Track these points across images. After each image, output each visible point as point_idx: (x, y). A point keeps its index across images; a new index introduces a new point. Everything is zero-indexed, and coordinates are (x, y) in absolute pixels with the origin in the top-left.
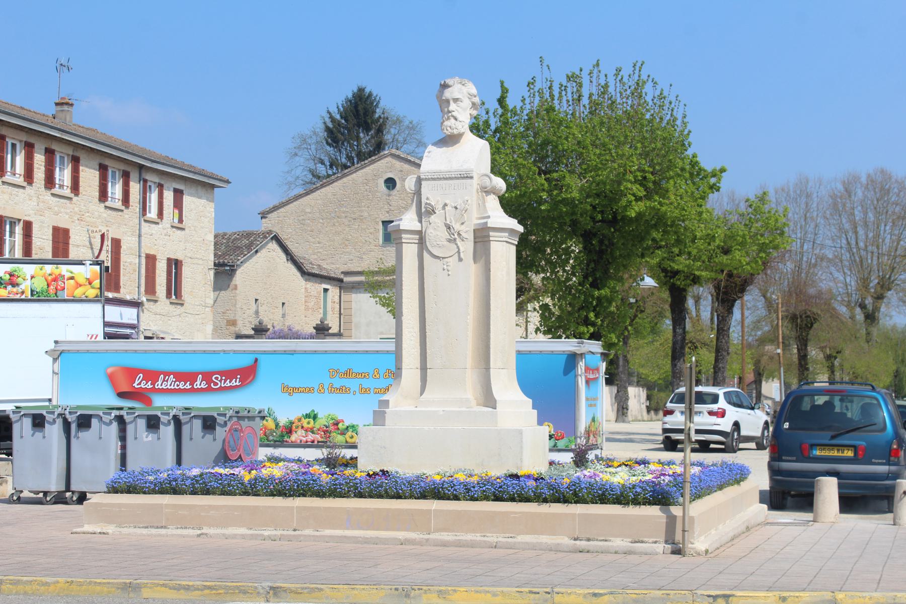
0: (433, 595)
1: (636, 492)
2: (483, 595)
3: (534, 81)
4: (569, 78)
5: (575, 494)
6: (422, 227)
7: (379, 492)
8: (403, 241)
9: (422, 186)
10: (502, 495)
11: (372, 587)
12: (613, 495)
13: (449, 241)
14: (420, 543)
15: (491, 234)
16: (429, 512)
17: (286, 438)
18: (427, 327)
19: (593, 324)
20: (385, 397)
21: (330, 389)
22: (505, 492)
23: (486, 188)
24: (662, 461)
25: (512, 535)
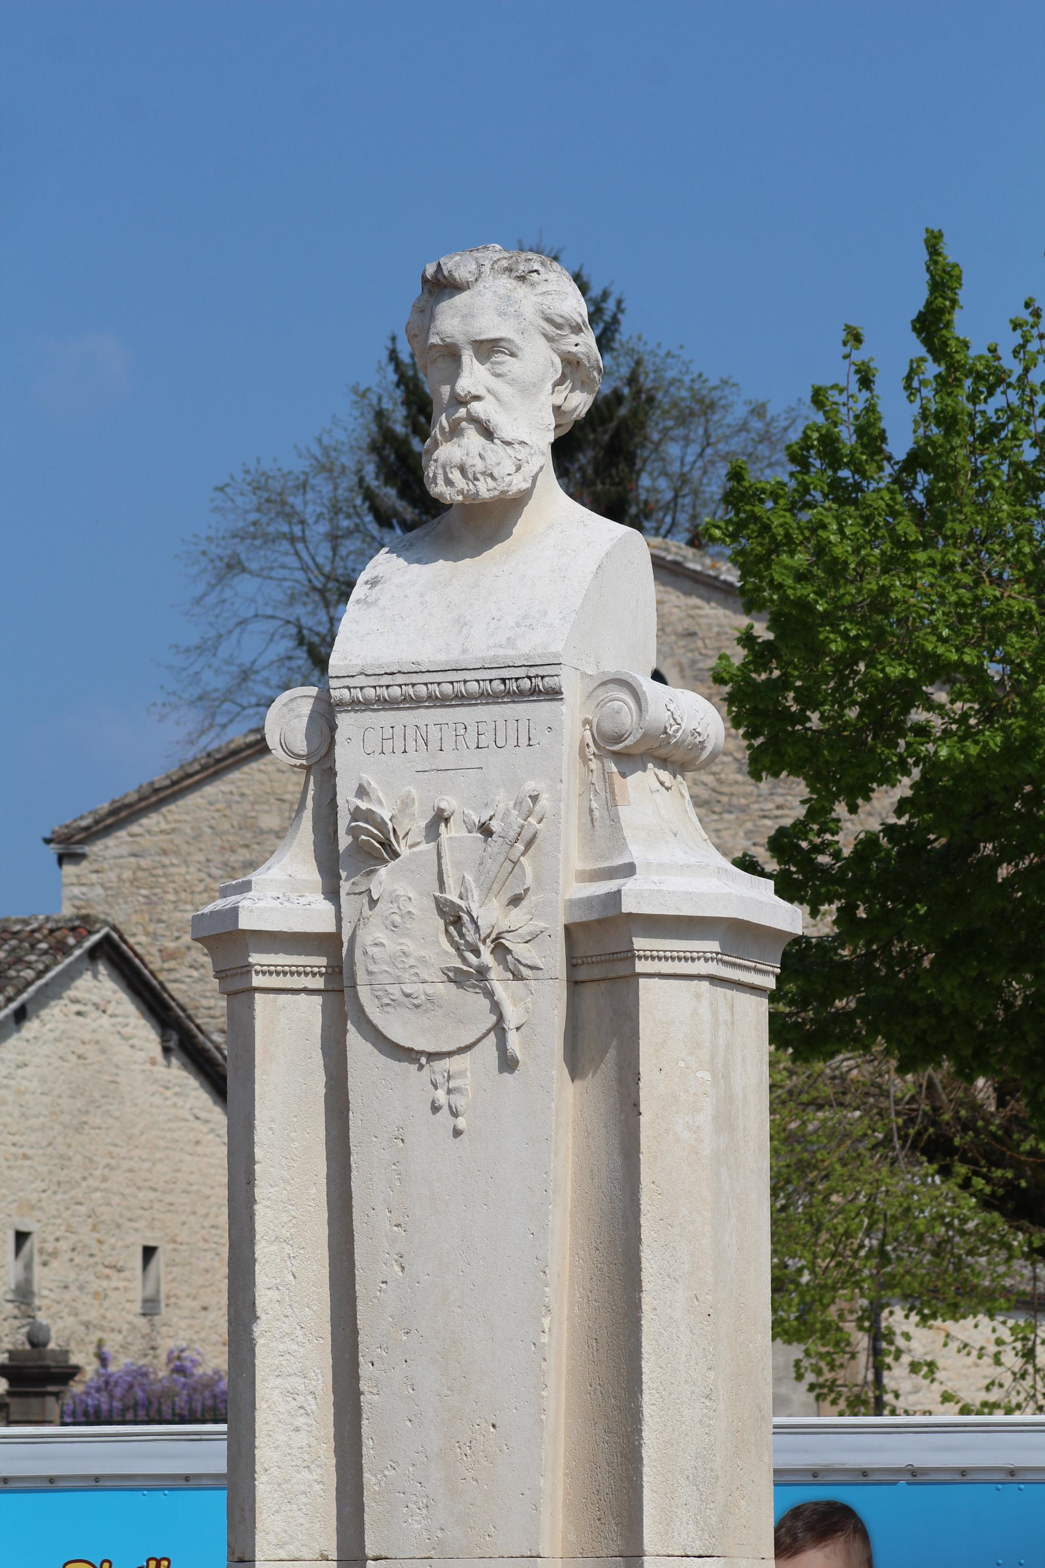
6: (339, 919)
8: (257, 981)
13: (458, 978)
15: (640, 943)
18: (365, 1370)
23: (619, 739)
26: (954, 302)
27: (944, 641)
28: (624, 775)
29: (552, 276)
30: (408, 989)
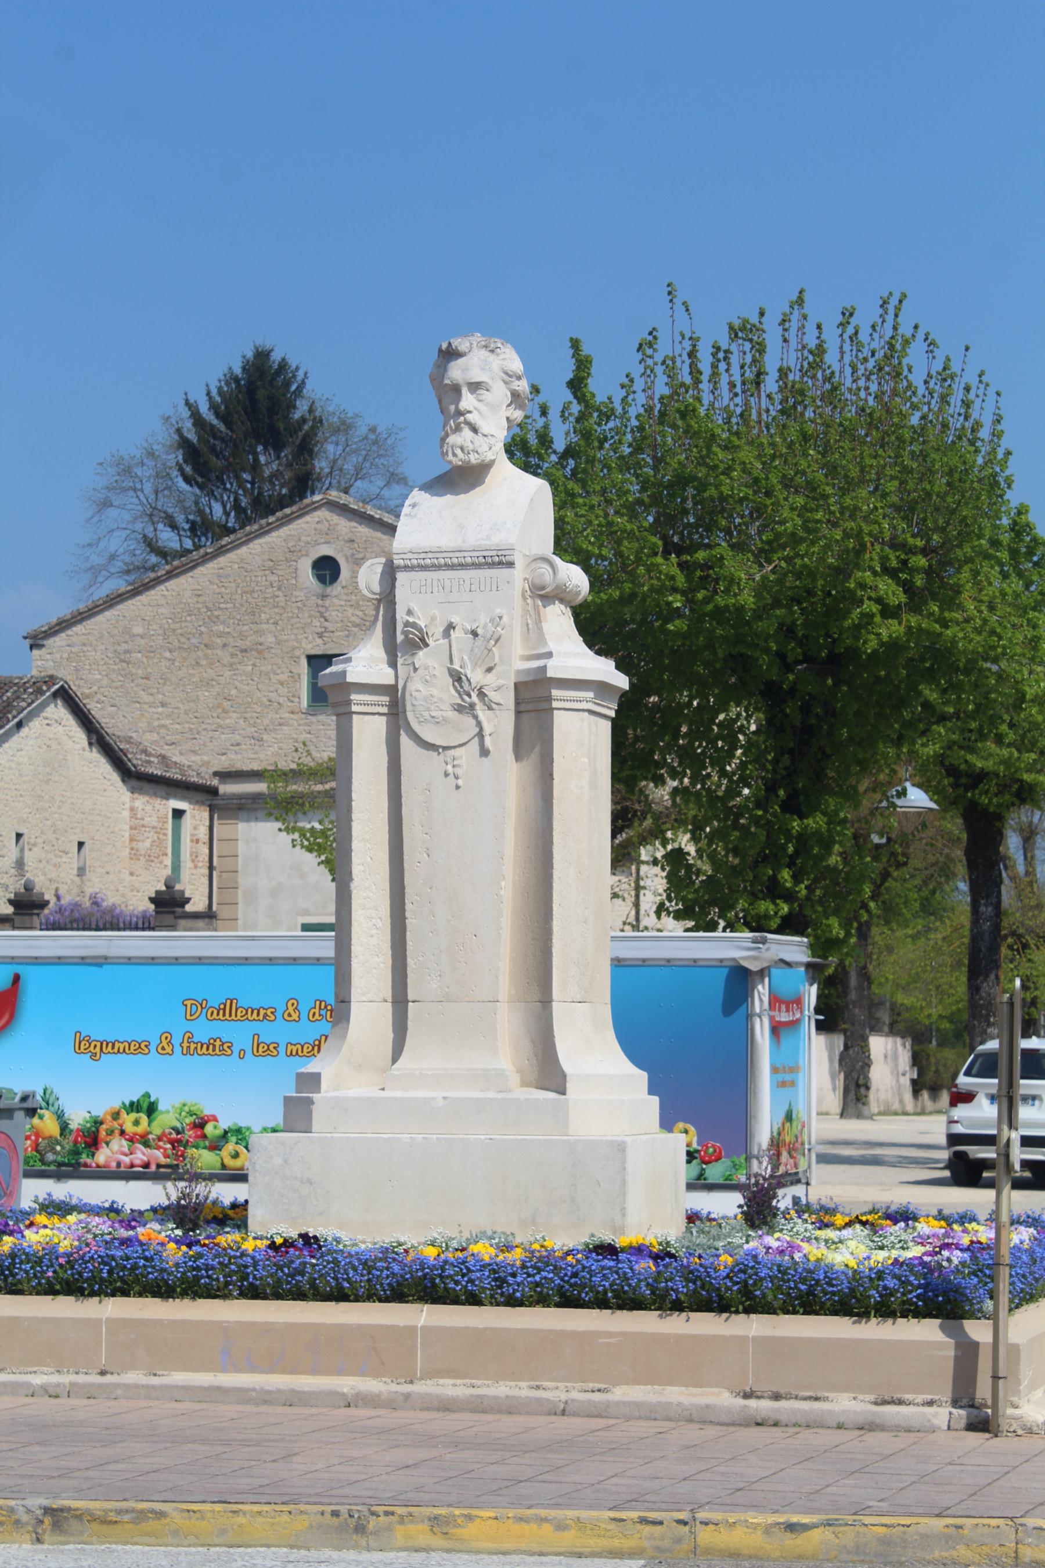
0: (420, 1527)
1: (885, 1288)
2: (533, 1526)
3: (655, 338)
4: (734, 333)
5: (746, 1291)
7: (296, 1285)
8: (354, 708)
9: (397, 584)
10: (579, 1294)
11: (278, 1508)
12: (833, 1293)
13: (459, 709)
14: (391, 1404)
15: (555, 693)
16: (411, 1330)
17: (84, 1158)
18: (408, 906)
19: (789, 896)
20: (312, 1066)
21: (185, 1045)
22: (583, 1286)
23: (543, 588)
24: (946, 1212)
25: (602, 1386)
26: (589, 374)
27: (593, 544)
28: (545, 607)
29: (507, 350)
30: (433, 714)
